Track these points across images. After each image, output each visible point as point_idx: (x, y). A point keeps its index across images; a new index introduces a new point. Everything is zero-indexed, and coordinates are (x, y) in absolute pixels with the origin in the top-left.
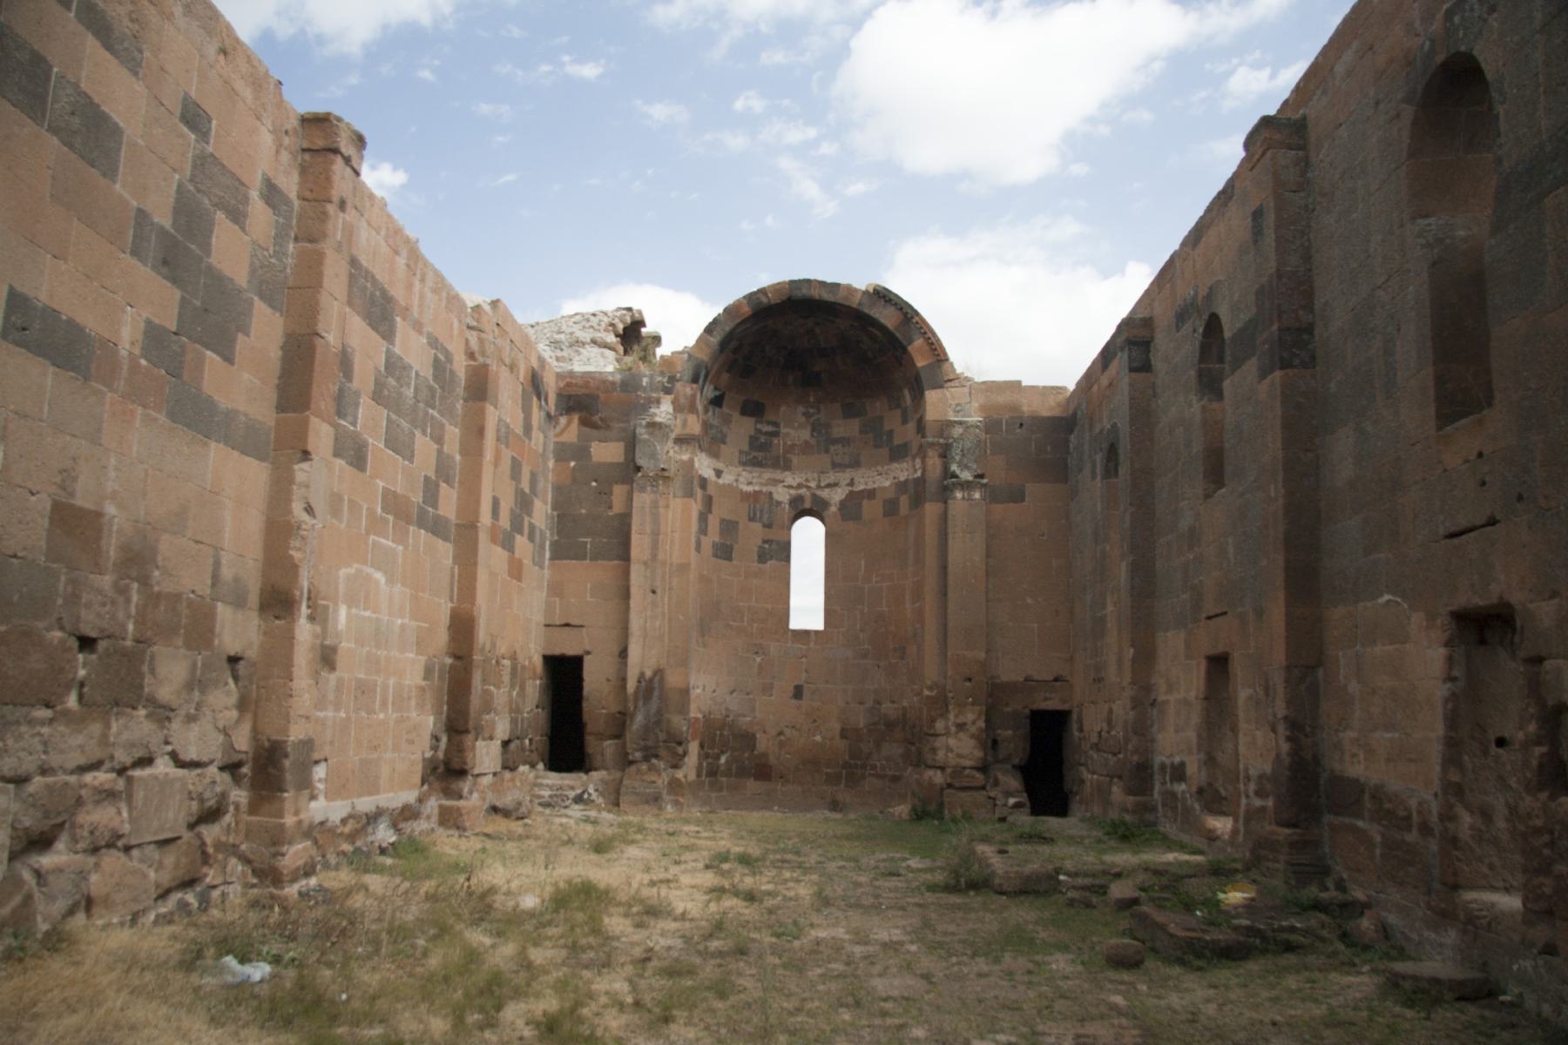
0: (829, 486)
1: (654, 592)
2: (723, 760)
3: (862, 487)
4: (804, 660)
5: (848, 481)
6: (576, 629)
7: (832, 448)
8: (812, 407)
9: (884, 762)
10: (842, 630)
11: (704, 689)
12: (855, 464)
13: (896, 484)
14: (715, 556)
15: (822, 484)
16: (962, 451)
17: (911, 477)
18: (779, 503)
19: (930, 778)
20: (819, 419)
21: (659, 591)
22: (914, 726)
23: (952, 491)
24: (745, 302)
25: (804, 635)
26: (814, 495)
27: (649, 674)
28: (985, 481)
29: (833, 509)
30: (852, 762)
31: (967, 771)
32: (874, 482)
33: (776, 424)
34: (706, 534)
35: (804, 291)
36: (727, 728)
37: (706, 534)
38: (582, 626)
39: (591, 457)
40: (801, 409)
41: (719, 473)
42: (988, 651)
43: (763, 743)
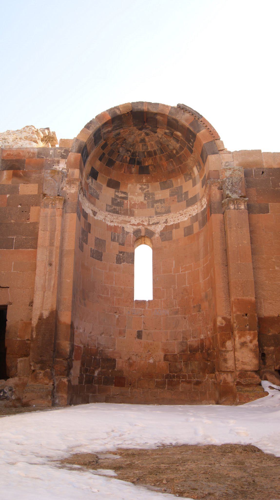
0: (153, 224)
1: (50, 265)
2: (96, 373)
3: (172, 223)
4: (143, 316)
5: (165, 221)
6: (3, 289)
7: (155, 205)
8: (145, 185)
9: (191, 373)
10: (163, 299)
11: (84, 331)
12: (168, 212)
13: (191, 217)
14: (93, 257)
15: (151, 223)
16: (232, 183)
17: (199, 212)
18: (128, 233)
19: (225, 379)
20: (148, 191)
21: (54, 264)
22: (209, 349)
23: (228, 205)
24: (108, 113)
25: (142, 303)
26: (146, 229)
27: (46, 314)
28: (247, 199)
29: (157, 235)
30: (171, 374)
31: (249, 373)
32: (178, 220)
33: (125, 193)
34: (87, 244)
35: (139, 107)
36: (98, 355)
37: (87, 244)
38: (9, 288)
39: (19, 192)
40: (139, 186)
41: (95, 213)
42: (256, 298)
43: (120, 364)
